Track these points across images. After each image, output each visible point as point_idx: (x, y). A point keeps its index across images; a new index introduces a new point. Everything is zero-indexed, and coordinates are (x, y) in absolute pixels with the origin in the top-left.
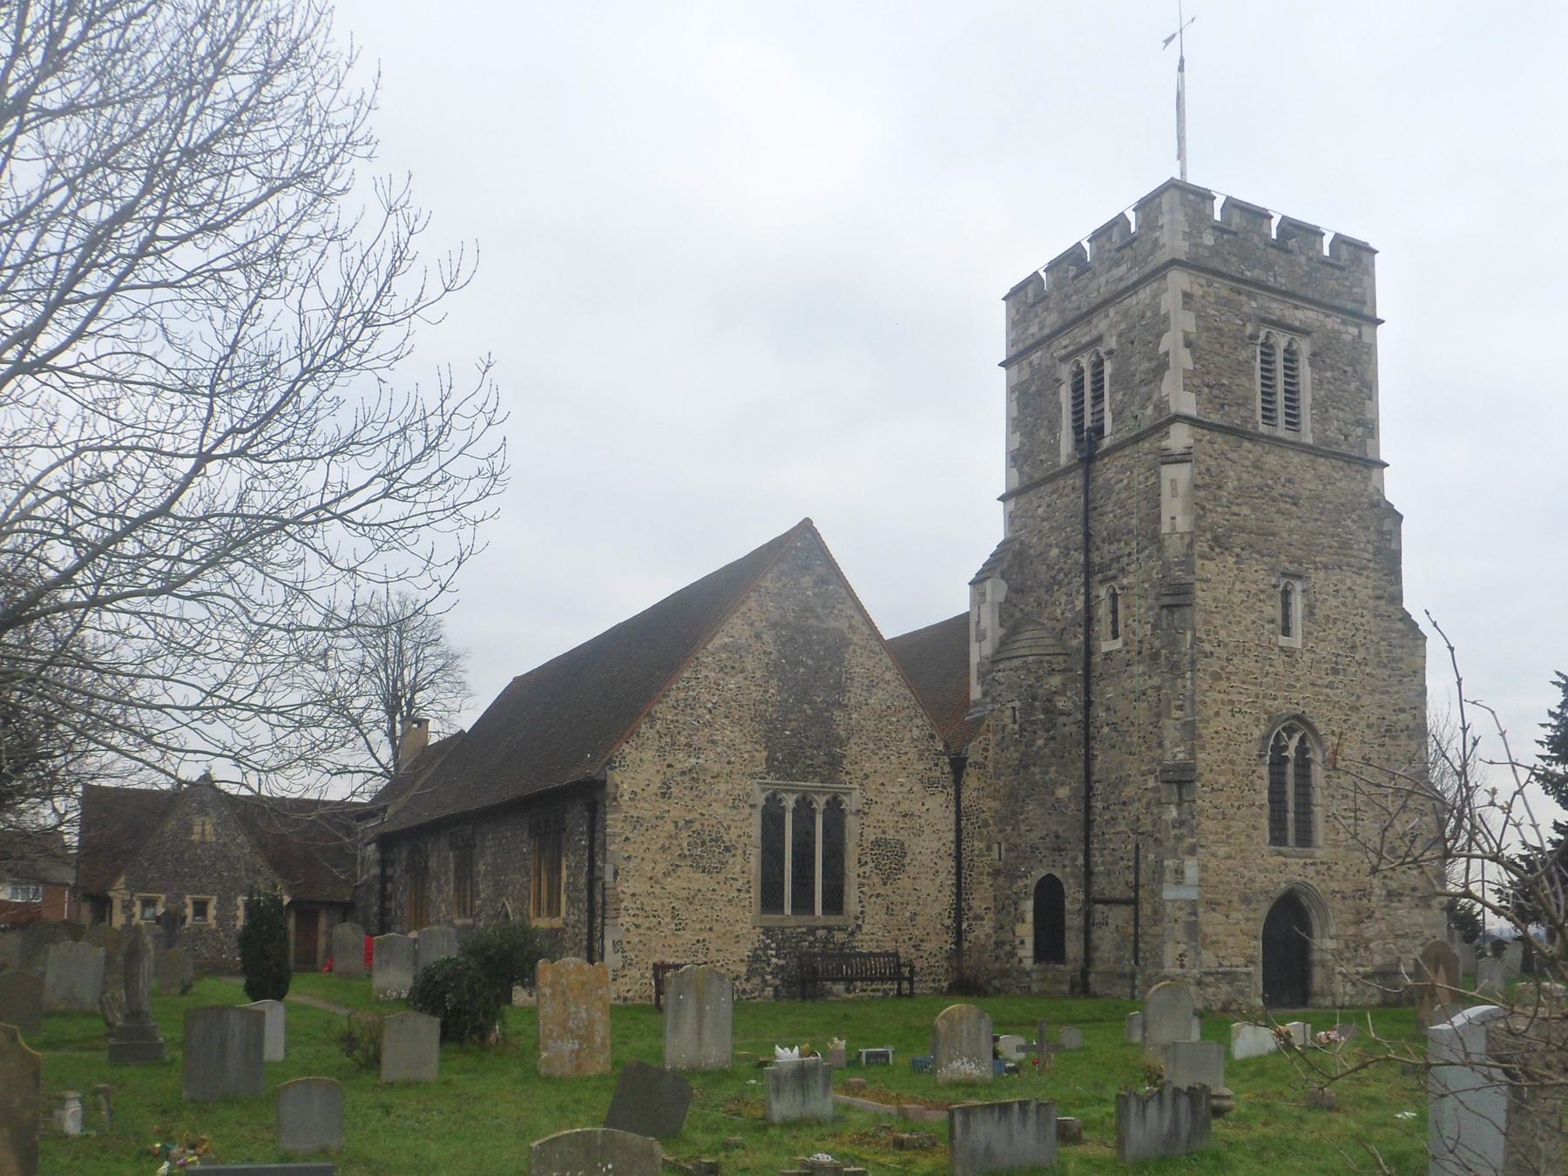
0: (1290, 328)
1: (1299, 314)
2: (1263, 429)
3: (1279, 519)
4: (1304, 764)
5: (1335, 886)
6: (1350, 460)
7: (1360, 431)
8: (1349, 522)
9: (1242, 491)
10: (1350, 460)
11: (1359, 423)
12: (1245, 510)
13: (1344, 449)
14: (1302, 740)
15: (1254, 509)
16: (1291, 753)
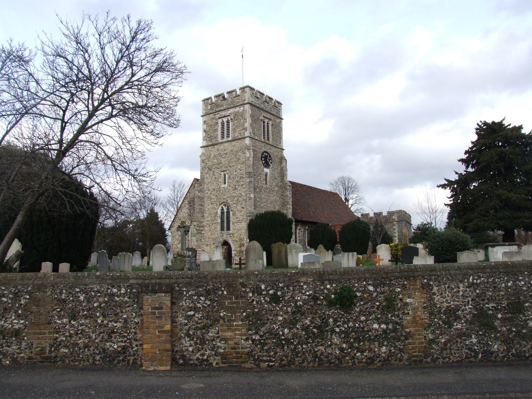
0: (225, 117)
1: (229, 112)
2: (220, 141)
3: (223, 160)
4: (228, 212)
5: (234, 239)
6: (239, 139)
7: (243, 131)
8: (240, 154)
9: (215, 156)
10: (239, 139)
11: (243, 129)
12: (215, 160)
13: (240, 137)
14: (228, 207)
15: (217, 159)
16: (225, 210)
